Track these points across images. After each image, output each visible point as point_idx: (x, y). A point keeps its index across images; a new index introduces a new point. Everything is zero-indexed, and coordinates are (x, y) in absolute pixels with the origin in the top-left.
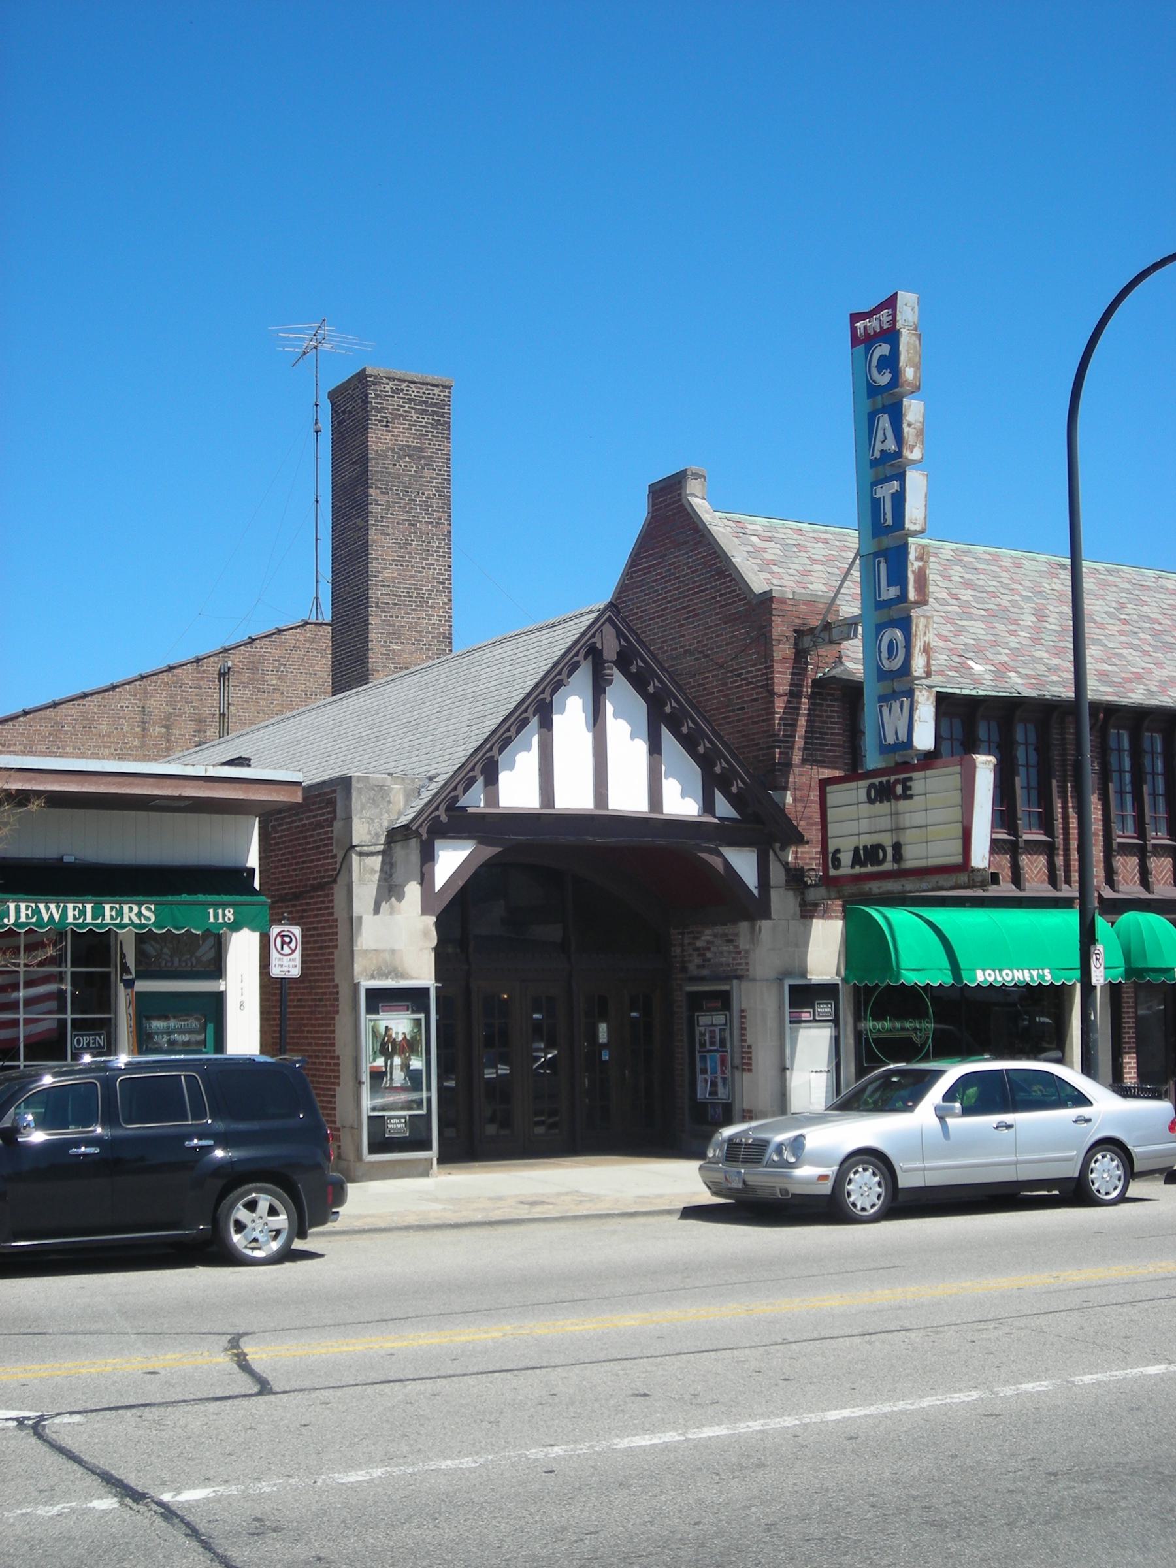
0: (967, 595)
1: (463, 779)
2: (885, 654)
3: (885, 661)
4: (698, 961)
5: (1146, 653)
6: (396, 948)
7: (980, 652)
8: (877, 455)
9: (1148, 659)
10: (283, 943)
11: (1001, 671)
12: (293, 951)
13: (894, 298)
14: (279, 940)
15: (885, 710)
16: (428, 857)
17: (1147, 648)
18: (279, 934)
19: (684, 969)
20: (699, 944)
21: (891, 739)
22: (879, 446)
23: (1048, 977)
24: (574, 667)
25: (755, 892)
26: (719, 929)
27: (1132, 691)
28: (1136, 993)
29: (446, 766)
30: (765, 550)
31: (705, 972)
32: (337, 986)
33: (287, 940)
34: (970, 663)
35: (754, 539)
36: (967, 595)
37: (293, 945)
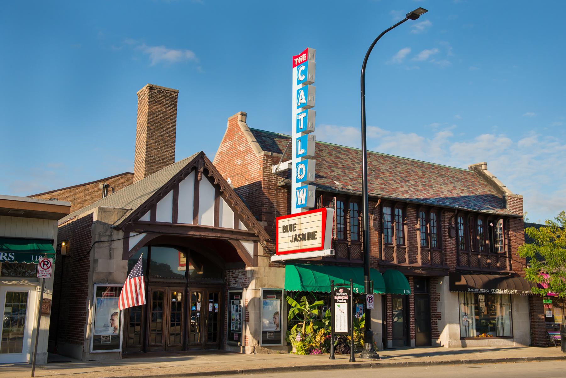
0: (337, 161)
1: (142, 210)
2: (299, 173)
3: (299, 176)
4: (233, 281)
5: (398, 183)
6: (111, 271)
7: (338, 179)
8: (299, 104)
9: (398, 184)
10: (44, 264)
11: (345, 184)
12: (49, 268)
13: (307, 49)
14: (42, 263)
15: (298, 193)
16: (126, 239)
17: (398, 181)
18: (43, 261)
19: (229, 285)
20: (234, 276)
21: (300, 203)
22: (300, 101)
23: (357, 291)
24: (187, 174)
25: (253, 257)
26: (240, 270)
27: (391, 194)
28: (392, 298)
29: (135, 206)
30: (266, 141)
31: (236, 285)
32: (88, 286)
33: (46, 263)
34: (335, 182)
35: (263, 138)
36: (337, 161)
37: (49, 266)
